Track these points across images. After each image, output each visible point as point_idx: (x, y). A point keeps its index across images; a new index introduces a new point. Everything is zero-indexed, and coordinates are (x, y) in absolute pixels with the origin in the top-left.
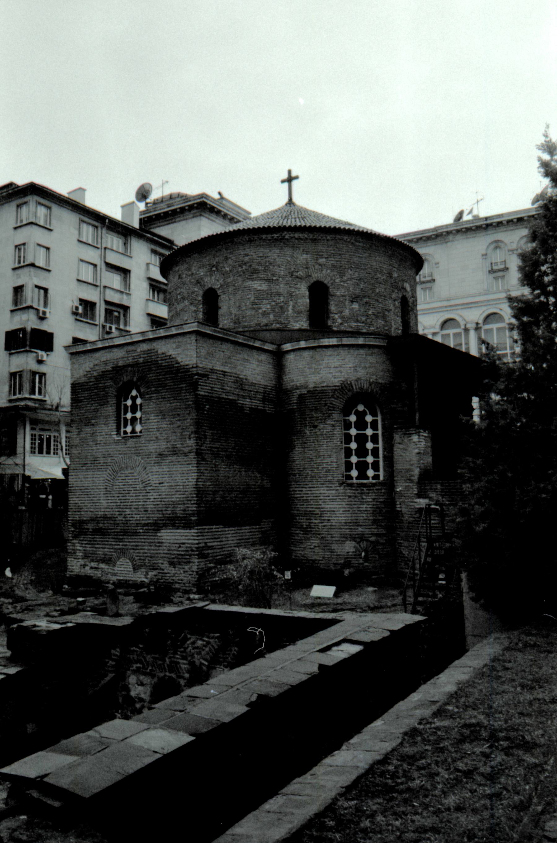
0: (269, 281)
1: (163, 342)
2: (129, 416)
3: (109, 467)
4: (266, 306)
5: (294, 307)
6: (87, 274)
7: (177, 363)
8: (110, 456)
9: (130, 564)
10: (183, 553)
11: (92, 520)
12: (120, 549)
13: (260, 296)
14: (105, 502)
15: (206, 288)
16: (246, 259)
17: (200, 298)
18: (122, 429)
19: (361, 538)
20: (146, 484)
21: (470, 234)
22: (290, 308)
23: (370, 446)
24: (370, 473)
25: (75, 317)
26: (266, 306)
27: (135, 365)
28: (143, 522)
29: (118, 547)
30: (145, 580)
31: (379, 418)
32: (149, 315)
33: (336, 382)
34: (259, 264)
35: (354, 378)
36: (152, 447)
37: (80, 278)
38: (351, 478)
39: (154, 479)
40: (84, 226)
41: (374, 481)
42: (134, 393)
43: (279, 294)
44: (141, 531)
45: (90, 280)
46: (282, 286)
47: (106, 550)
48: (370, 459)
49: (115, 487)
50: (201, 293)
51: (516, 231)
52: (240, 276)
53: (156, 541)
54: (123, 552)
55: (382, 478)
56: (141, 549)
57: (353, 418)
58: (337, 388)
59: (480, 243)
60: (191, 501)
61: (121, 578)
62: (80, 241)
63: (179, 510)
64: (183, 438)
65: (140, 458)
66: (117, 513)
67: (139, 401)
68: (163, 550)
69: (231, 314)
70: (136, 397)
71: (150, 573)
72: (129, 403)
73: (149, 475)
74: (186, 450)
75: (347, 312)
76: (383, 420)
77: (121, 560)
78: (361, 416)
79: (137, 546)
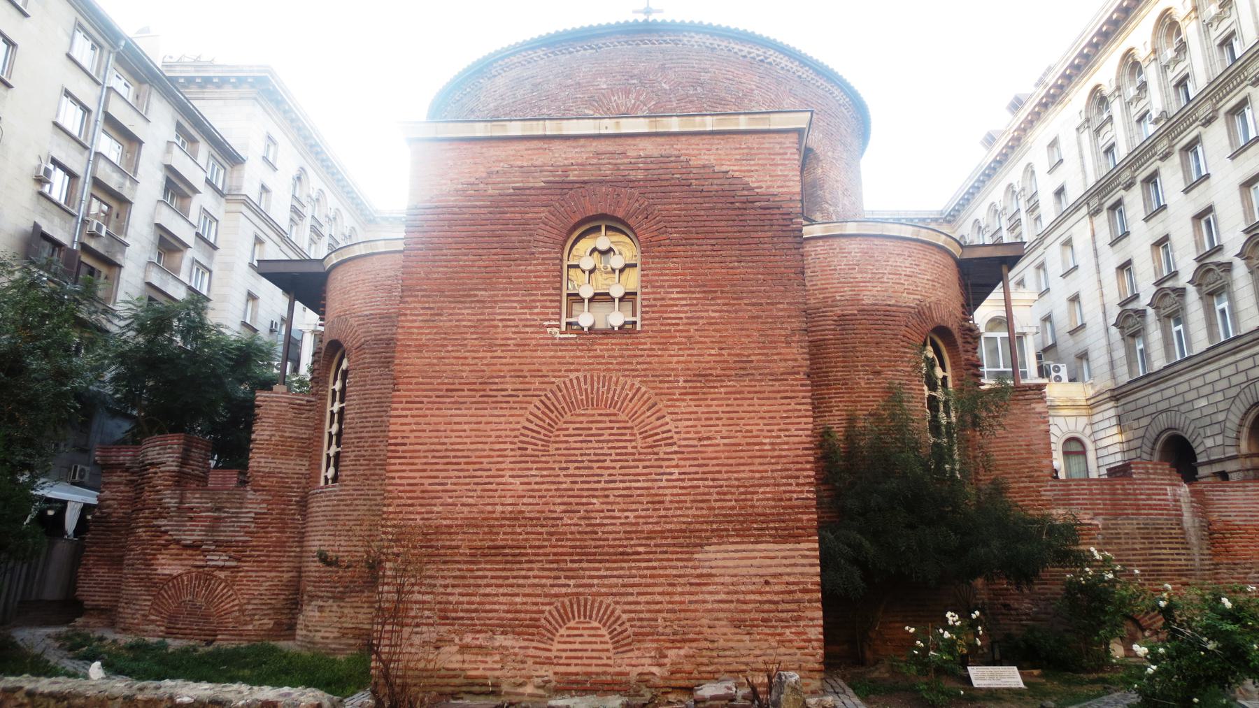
1: (702, 143)
3: (536, 401)
6: (71, 118)
8: (537, 373)
9: (603, 631)
10: (776, 598)
11: (472, 523)
12: (566, 595)
14: (517, 481)
18: (564, 320)
20: (655, 440)
25: (38, 188)
27: (620, 183)
28: (645, 528)
29: (563, 590)
30: (655, 669)
31: (949, 374)
32: (159, 226)
33: (910, 300)
36: (675, 357)
37: (60, 121)
40: (79, 36)
44: (641, 549)
45: (76, 133)
47: (518, 599)
54: (578, 607)
56: (639, 594)
60: (798, 477)
61: (572, 669)
62: (69, 56)
63: (762, 499)
65: (637, 382)
66: (559, 508)
68: (711, 596)
71: (672, 653)
73: (667, 419)
74: (781, 367)
76: (958, 378)
77: (572, 624)
78: (931, 365)
79: (624, 586)
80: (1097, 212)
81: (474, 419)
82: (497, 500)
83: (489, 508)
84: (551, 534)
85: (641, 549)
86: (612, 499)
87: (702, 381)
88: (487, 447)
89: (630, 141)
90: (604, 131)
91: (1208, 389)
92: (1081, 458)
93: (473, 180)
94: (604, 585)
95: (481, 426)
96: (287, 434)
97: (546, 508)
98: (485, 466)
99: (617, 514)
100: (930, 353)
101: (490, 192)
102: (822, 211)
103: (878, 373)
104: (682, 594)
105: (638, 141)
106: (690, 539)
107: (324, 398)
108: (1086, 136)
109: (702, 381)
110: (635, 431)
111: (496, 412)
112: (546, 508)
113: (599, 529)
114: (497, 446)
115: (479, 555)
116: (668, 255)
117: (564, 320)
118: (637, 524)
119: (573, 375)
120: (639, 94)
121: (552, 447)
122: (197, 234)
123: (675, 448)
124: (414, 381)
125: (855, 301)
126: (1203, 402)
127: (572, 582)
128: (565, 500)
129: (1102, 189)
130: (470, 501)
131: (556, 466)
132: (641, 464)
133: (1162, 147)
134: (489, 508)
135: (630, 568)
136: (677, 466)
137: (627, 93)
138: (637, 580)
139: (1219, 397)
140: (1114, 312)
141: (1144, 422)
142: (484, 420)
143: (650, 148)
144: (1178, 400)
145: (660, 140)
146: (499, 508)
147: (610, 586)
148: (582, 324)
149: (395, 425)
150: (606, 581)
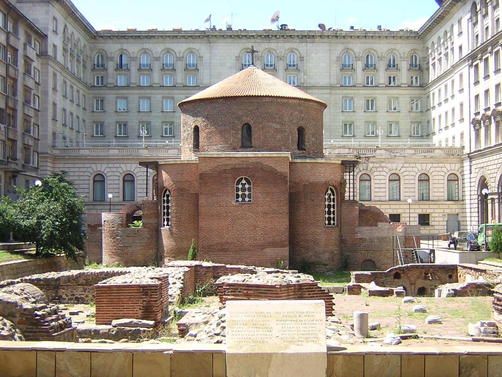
0: (281, 124)
4: (279, 137)
7: (276, 170)
8: (230, 212)
11: (217, 244)
13: (277, 131)
19: (332, 252)
20: (255, 227)
21: (229, 40)
22: (290, 139)
23: (332, 210)
24: (332, 222)
26: (279, 137)
31: (335, 197)
33: (323, 180)
34: (276, 114)
38: (326, 224)
43: (286, 131)
48: (332, 216)
51: (262, 44)
52: (266, 119)
55: (336, 224)
57: (327, 197)
59: (235, 49)
67: (247, 186)
69: (260, 138)
70: (245, 184)
72: (240, 186)
74: (281, 212)
76: (337, 198)
80: (471, 66)
91: (493, 163)
92: (457, 182)
100: (329, 192)
101: (218, 170)
103: (313, 200)
106: (262, 247)
108: (470, 24)
115: (219, 250)
116: (258, 186)
117: (236, 199)
122: (36, 82)
126: (491, 167)
129: (472, 57)
133: (490, 49)
137: (247, 116)
139: (495, 167)
140: (473, 116)
141: (477, 170)
143: (254, 160)
144: (485, 164)
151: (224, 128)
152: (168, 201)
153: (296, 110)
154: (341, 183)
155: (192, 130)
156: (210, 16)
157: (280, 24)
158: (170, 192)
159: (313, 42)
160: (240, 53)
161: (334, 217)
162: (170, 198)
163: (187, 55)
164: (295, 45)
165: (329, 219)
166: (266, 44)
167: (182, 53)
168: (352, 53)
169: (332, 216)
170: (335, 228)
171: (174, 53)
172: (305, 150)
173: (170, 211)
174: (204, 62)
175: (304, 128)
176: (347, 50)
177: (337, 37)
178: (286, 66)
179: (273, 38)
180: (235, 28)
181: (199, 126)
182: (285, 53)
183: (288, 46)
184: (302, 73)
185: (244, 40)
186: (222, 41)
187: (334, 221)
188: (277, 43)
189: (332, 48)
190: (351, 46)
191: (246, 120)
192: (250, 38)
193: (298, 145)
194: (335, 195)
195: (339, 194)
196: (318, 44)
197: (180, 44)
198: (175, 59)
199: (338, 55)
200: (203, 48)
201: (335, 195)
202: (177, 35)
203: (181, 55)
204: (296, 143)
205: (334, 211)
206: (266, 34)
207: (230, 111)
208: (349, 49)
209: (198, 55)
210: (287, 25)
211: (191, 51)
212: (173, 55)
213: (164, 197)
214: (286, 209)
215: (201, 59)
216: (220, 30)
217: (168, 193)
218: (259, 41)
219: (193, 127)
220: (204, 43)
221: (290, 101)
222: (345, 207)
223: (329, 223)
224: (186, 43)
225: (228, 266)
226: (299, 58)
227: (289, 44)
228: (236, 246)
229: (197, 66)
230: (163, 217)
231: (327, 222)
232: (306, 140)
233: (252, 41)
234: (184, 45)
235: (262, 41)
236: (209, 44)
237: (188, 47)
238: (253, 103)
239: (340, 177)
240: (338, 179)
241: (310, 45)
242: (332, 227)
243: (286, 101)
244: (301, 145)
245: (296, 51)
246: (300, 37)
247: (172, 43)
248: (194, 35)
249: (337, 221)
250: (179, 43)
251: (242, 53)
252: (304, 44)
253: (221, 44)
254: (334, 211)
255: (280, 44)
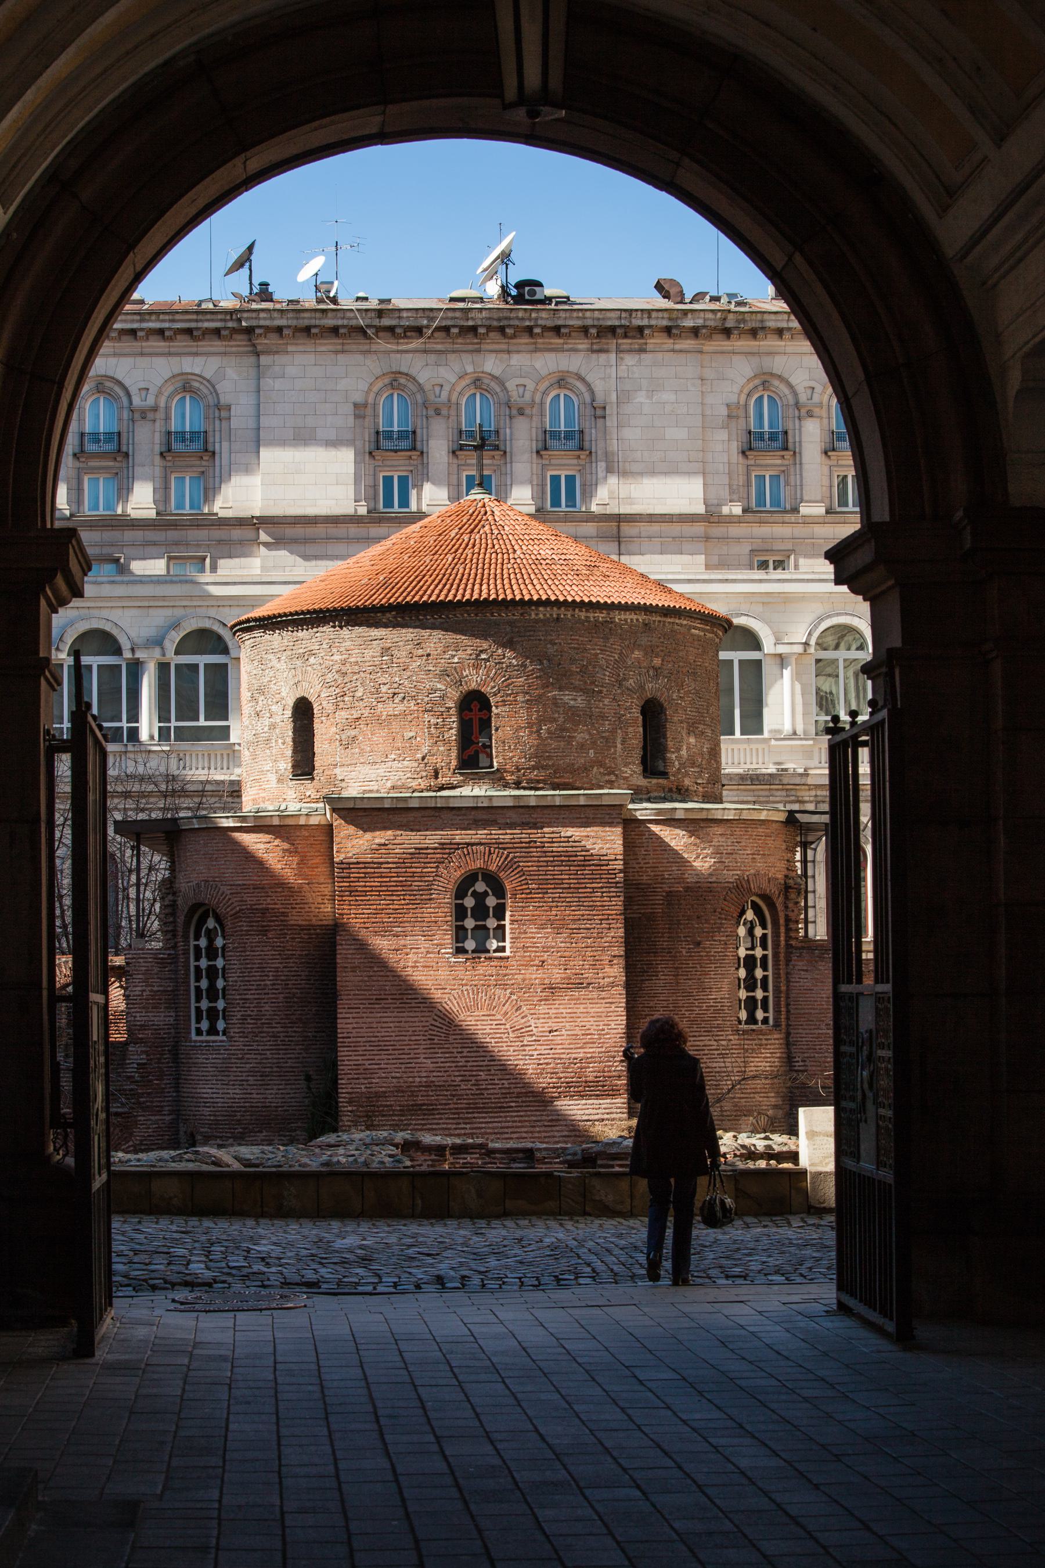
2: (470, 923)
5: (623, 742)
11: (399, 1090)
14: (429, 1061)
15: (465, 688)
16: (551, 650)
17: (451, 704)
22: (619, 741)
23: (759, 973)
24: (760, 1015)
28: (515, 1090)
31: (769, 931)
35: (752, 871)
38: (740, 1022)
39: (537, 1026)
41: (763, 1027)
42: (480, 887)
43: (603, 717)
44: (513, 1104)
46: (606, 701)
49: (451, 1037)
50: (454, 695)
51: (451, 357)
53: (544, 1118)
58: (731, 885)
64: (597, 964)
67: (491, 901)
70: (486, 894)
75: (684, 752)
79: (502, 1128)
81: (397, 1020)
82: (416, 1074)
83: (411, 1079)
84: (454, 1096)
85: (513, 1104)
86: (493, 1072)
87: (552, 989)
88: (407, 1038)
89: (500, 811)
90: (480, 805)
93: (383, 841)
94: (489, 1128)
95: (402, 1024)
96: (155, 989)
97: (449, 1079)
98: (406, 1051)
99: (496, 1082)
100: (750, 915)
102: (664, 759)
103: (699, 944)
104: (539, 1132)
105: (505, 811)
107: (186, 952)
109: (552, 989)
110: (508, 1026)
111: (411, 1014)
112: (449, 1079)
113: (485, 1092)
114: (413, 1038)
118: (509, 1088)
119: (464, 988)
120: (489, 670)
121: (451, 1037)
123: (534, 1038)
124: (352, 993)
125: (681, 879)
127: (468, 1126)
128: (462, 1073)
130: (398, 1075)
131: (455, 1050)
132: (512, 1049)
134: (411, 1079)
135: (506, 1117)
136: (536, 1050)
138: (510, 1124)
142: (403, 1019)
145: (521, 810)
146: (418, 1079)
147: (493, 1128)
148: (467, 947)
149: (341, 1024)
150: (490, 1125)
151: (401, 707)
152: (212, 953)
153: (636, 646)
154: (787, 888)
155: (289, 713)
156: (250, 249)
157: (513, 280)
158: (218, 919)
159: (642, 350)
160: (370, 390)
161: (765, 999)
162: (219, 942)
163: (170, 397)
164: (575, 360)
165: (751, 1004)
166: (467, 358)
167: (153, 390)
168: (784, 389)
169: (759, 994)
170: (771, 1032)
171: (121, 393)
172: (664, 774)
173: (220, 983)
174: (234, 423)
175: (661, 706)
176: (765, 380)
177: (727, 332)
178: (541, 437)
179: (491, 334)
180: (346, 302)
181: (312, 699)
182: (536, 390)
183: (547, 363)
184: (602, 465)
185: (382, 344)
186: (301, 348)
187: (765, 1009)
188: (509, 352)
189: (709, 373)
190: (778, 364)
191: (474, 680)
192: (406, 337)
193: (644, 761)
194: (769, 926)
195: (782, 921)
196: (660, 355)
197: (148, 359)
198: (126, 414)
199: (734, 399)
200: (231, 373)
201: (769, 926)
202: (135, 326)
203: (151, 401)
204: (637, 754)
205: (765, 978)
206: (470, 323)
207: (420, 652)
208: (772, 374)
209: (211, 400)
210: (540, 285)
211: (186, 386)
212: (117, 398)
213: (197, 938)
214: (616, 972)
215: (224, 414)
216: (294, 308)
217: (211, 923)
218: (439, 347)
219: (290, 702)
220: (238, 354)
221: (618, 617)
222: (801, 965)
223: (752, 1019)
224: (170, 354)
225: (491, 1145)
226: (589, 411)
227: (550, 357)
228: (460, 1097)
229: (211, 440)
230: (193, 1005)
231: (743, 1015)
232: (670, 744)
233: (411, 346)
234: (160, 362)
235: (449, 347)
236: (252, 359)
237: (176, 371)
238: (497, 624)
239: (782, 865)
240: (778, 872)
241: (630, 360)
242: (761, 1032)
243: (601, 616)
244: (653, 758)
245: (579, 384)
246: (593, 331)
247: (115, 355)
248: (200, 325)
249: (777, 1012)
250: (142, 354)
251: (375, 389)
252: (603, 357)
253: (299, 359)
254: (765, 979)
255: (516, 359)
